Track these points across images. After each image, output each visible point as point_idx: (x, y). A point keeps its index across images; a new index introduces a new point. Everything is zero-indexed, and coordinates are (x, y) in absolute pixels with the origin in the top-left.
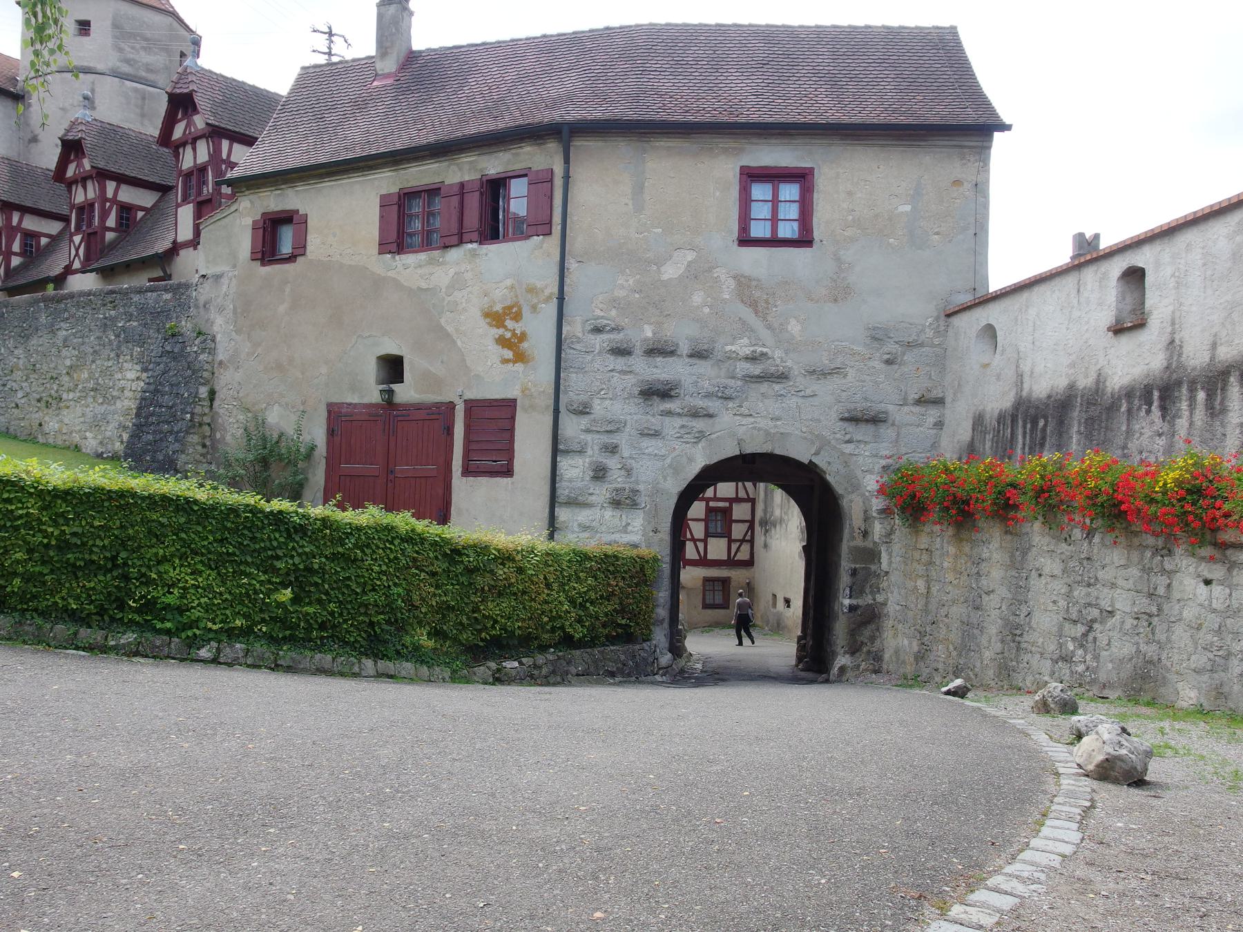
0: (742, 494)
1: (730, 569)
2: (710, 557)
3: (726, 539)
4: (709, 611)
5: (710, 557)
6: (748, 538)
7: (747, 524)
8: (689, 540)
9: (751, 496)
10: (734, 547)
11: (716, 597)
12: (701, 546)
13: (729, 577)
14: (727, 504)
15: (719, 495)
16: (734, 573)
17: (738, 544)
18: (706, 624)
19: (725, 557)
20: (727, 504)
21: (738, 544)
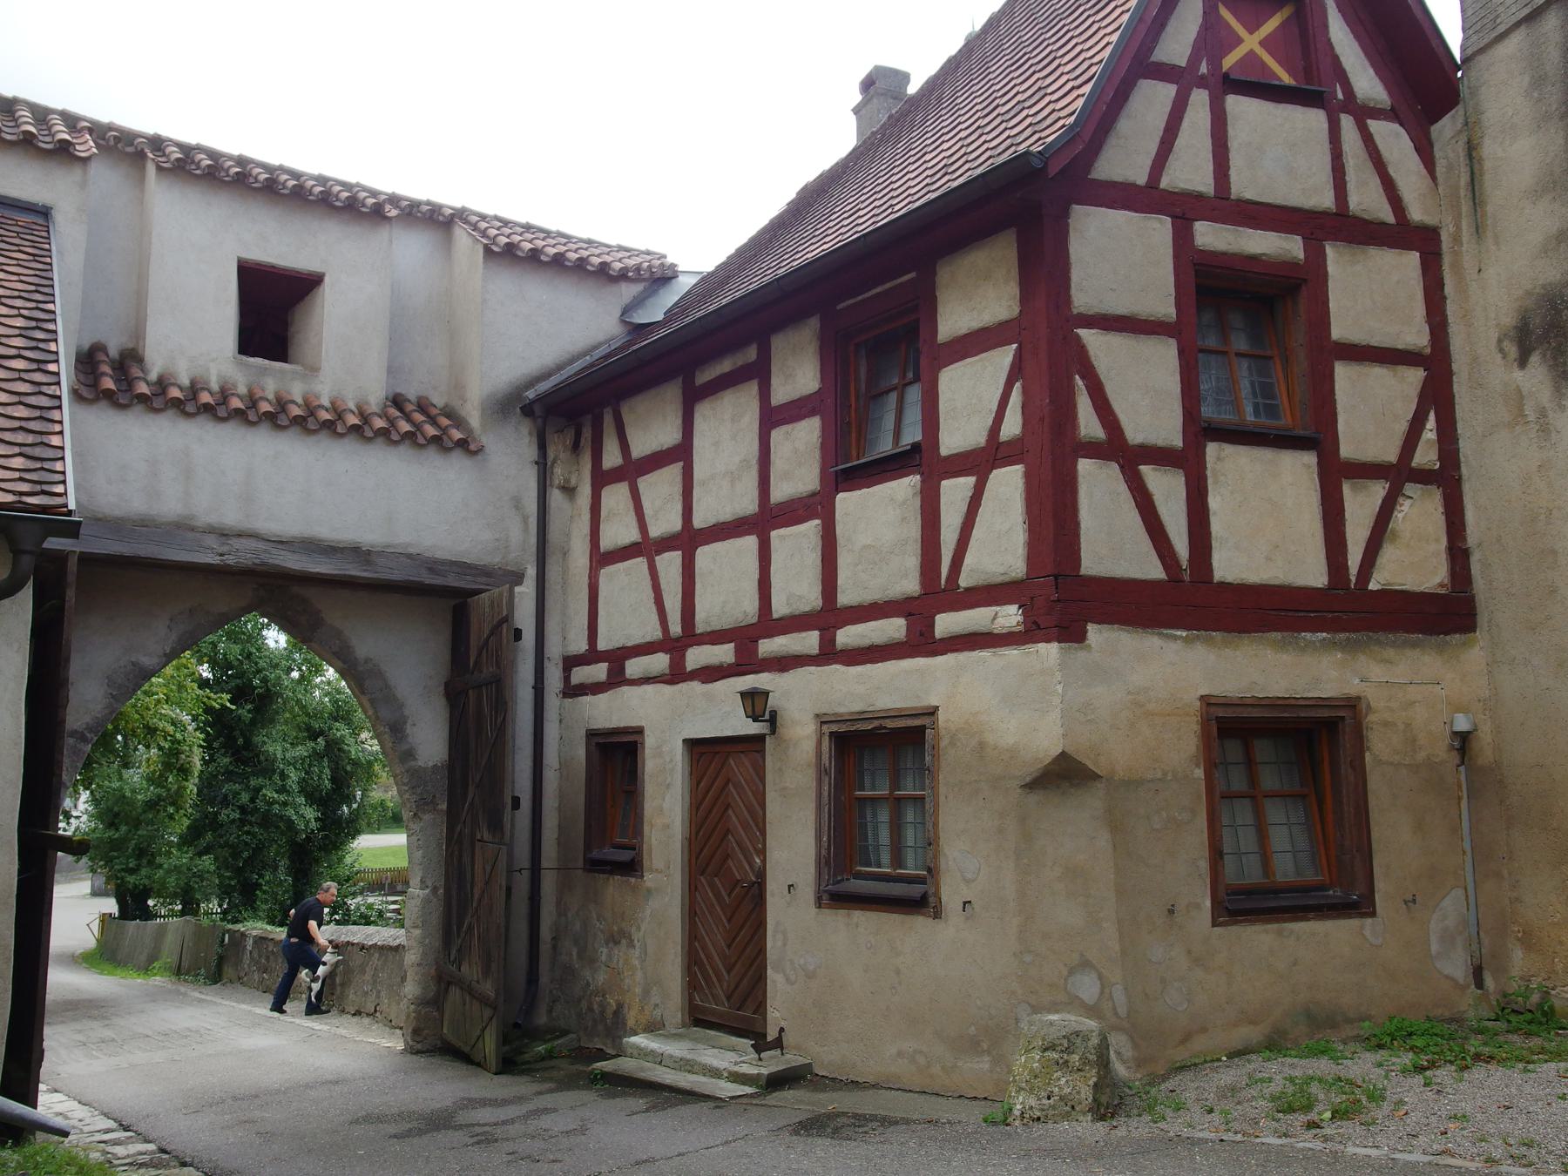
0: (1366, 199)
1: (1351, 648)
2: (1228, 565)
3: (1310, 459)
4: (1259, 938)
5: (1228, 565)
6: (1426, 455)
7: (1416, 376)
8: (1094, 450)
9: (1416, 214)
10: (1361, 504)
11: (1279, 838)
12: (1167, 487)
13: (1352, 705)
14: (1291, 247)
15: (1243, 186)
16: (1377, 672)
17: (1378, 491)
18: (1253, 1034)
19: (1314, 574)
20: (1291, 247)
21: (1378, 491)
